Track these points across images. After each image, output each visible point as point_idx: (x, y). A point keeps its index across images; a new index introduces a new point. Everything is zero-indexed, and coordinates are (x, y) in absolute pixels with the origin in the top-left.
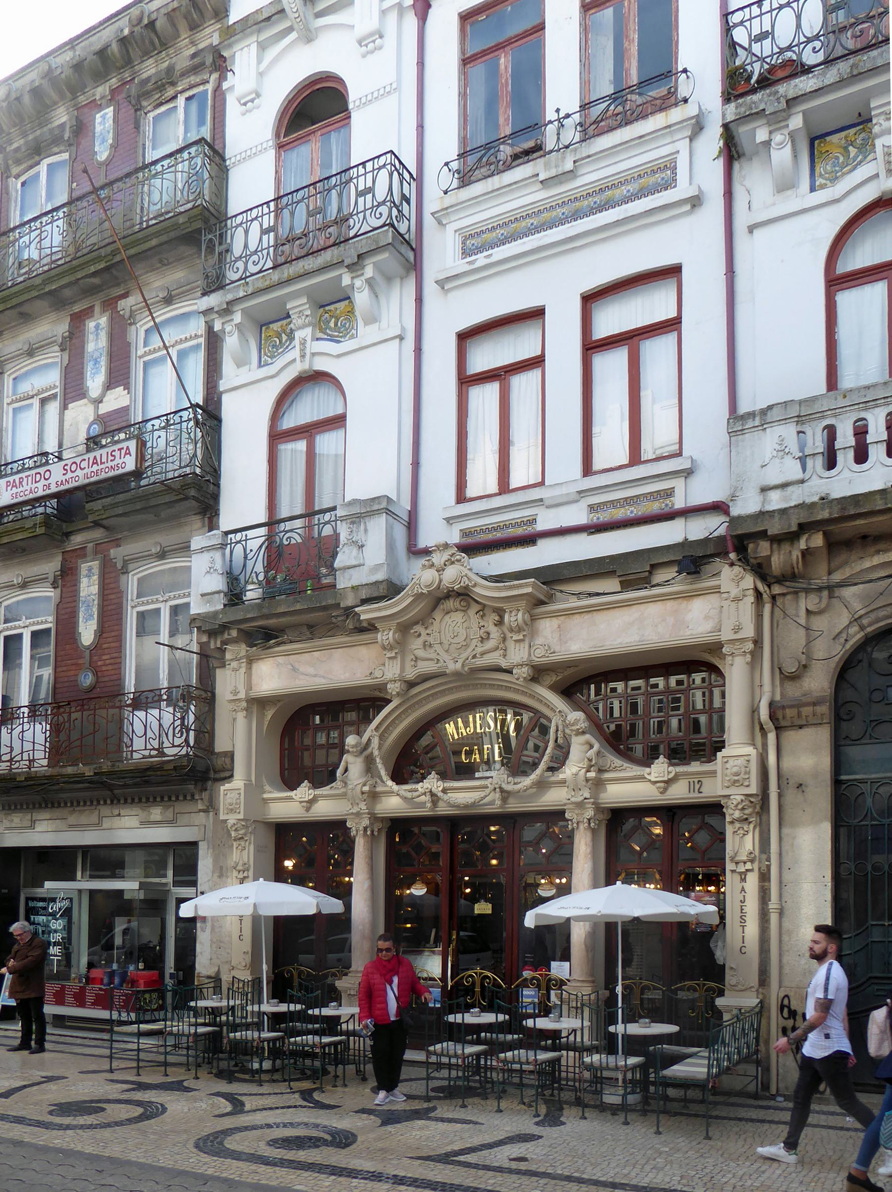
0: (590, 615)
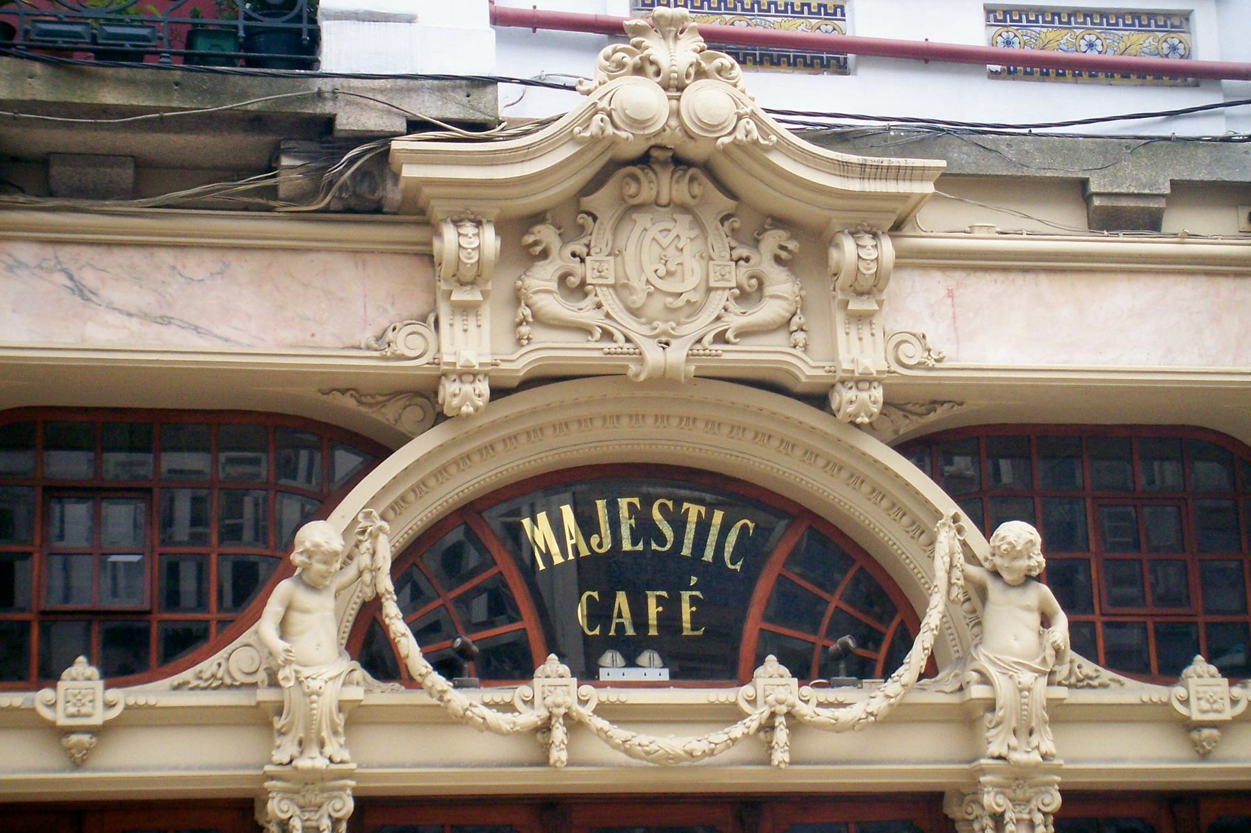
0: (1030, 277)
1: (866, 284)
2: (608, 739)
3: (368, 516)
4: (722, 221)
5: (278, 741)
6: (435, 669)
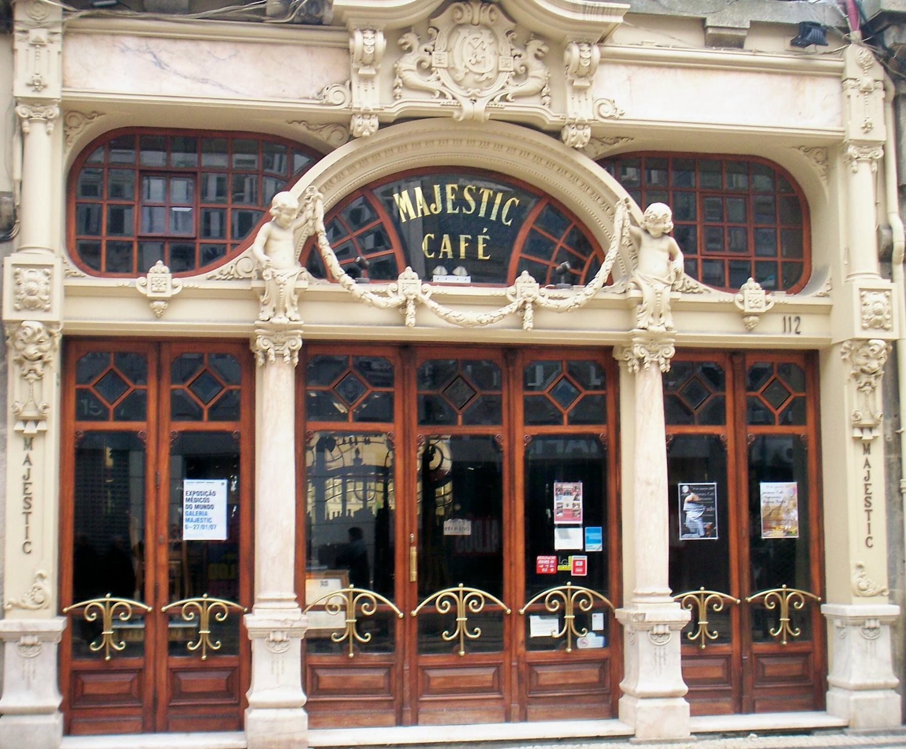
0: (672, 71)
1: (583, 71)
2: (437, 313)
3: (311, 190)
4: (508, 34)
5: (262, 308)
6: (346, 273)
